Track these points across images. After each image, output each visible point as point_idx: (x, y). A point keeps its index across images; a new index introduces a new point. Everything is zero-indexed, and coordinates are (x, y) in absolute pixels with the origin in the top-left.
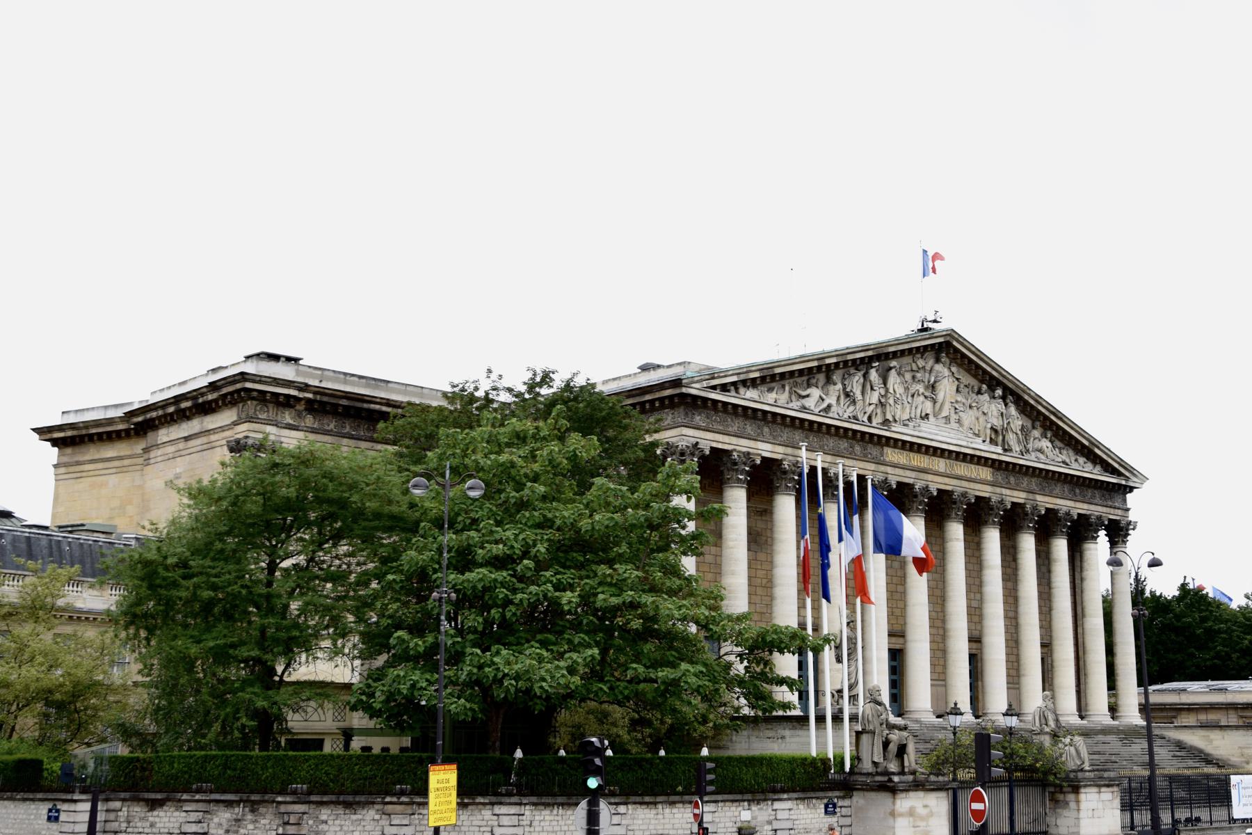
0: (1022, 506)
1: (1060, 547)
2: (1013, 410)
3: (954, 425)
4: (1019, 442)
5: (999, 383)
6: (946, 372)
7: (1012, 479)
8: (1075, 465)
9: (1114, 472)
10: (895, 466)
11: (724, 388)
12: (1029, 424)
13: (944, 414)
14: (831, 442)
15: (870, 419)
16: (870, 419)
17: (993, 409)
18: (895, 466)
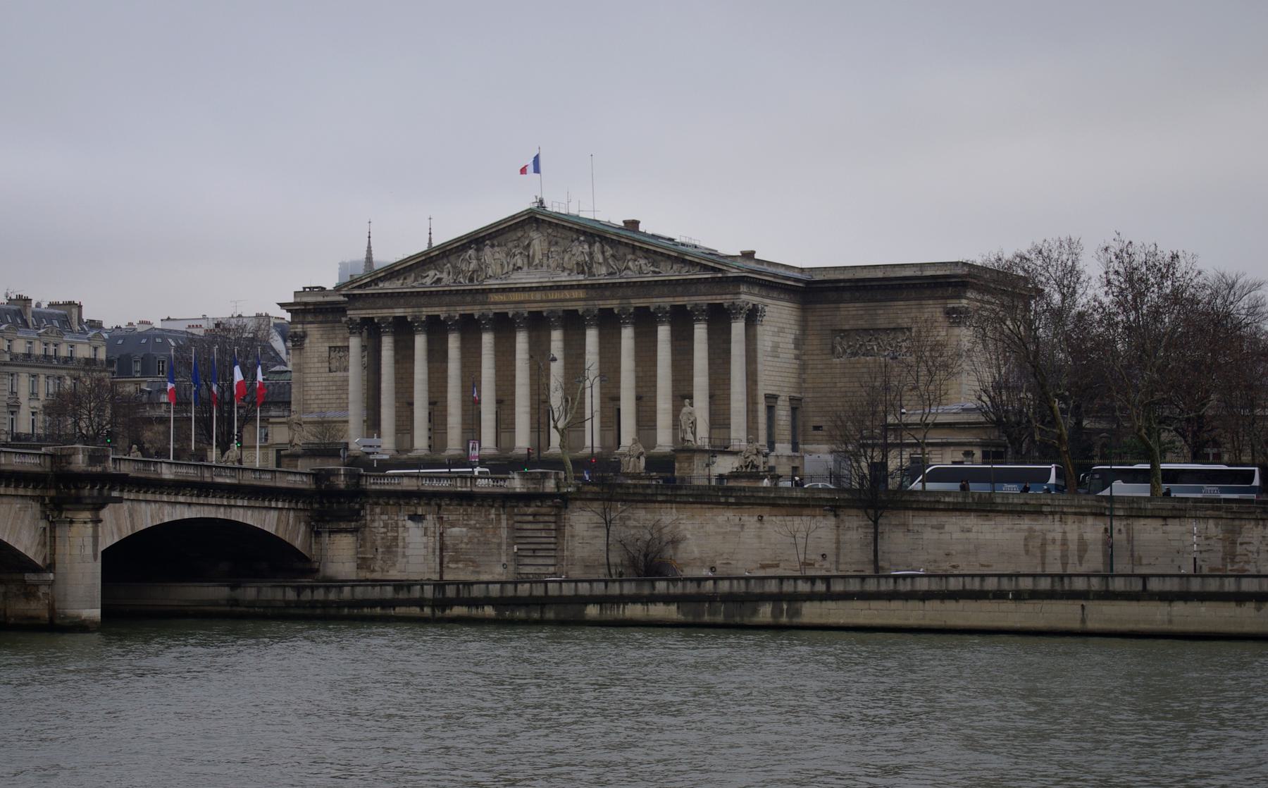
0: (612, 309)
1: (664, 332)
2: (597, 247)
3: (545, 268)
4: (608, 265)
5: (584, 233)
6: (534, 235)
7: (607, 293)
8: (671, 272)
9: (714, 269)
10: (495, 303)
11: (366, 285)
12: (628, 250)
13: (537, 261)
14: (447, 299)
15: (471, 280)
16: (471, 280)
17: (580, 250)
18: (495, 303)
